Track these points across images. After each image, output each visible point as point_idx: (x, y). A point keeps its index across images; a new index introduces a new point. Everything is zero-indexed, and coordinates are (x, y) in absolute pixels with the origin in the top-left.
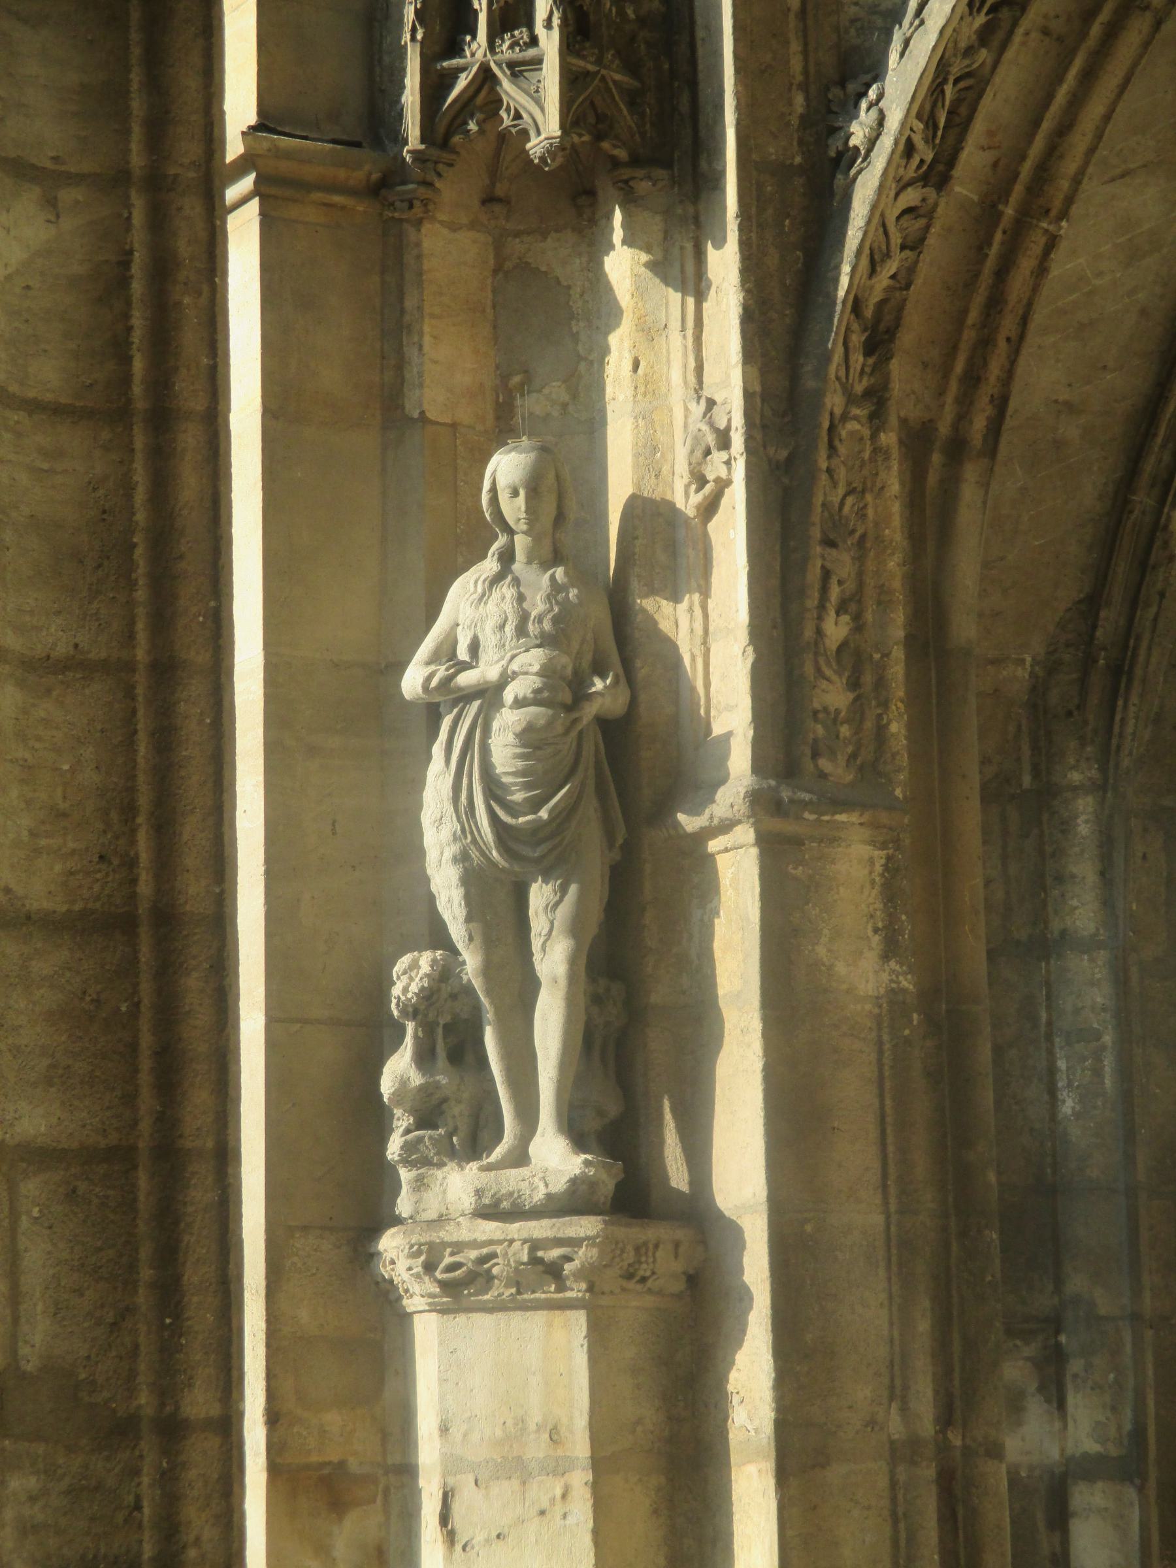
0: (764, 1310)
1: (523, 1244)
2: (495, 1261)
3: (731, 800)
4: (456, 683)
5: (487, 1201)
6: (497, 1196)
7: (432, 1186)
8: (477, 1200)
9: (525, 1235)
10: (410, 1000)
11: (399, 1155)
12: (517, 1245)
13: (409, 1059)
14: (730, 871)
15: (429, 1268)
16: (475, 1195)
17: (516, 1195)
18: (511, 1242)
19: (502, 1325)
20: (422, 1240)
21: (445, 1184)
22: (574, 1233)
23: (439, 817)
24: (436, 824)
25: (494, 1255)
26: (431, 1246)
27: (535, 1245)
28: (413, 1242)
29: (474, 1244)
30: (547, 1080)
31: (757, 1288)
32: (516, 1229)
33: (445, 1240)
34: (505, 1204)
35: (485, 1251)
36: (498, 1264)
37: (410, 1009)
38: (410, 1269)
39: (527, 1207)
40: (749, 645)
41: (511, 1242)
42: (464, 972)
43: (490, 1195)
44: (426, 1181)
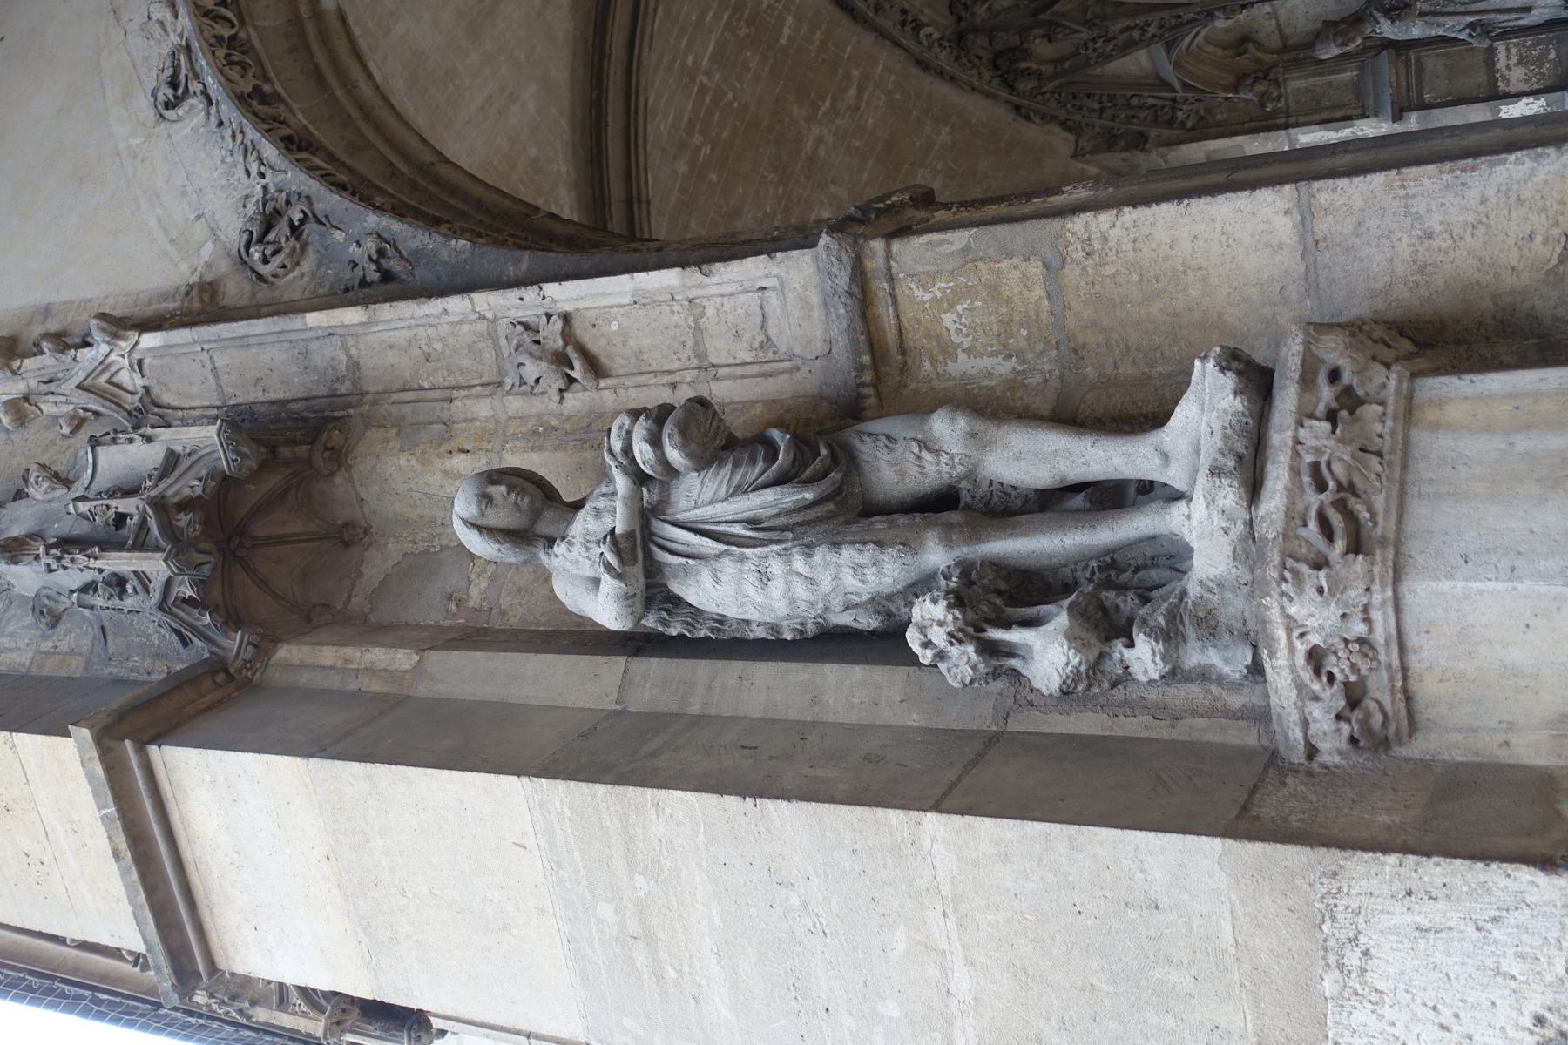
0: (1444, 177)
1: (1302, 426)
2: (1323, 466)
3: (834, 259)
4: (622, 535)
5: (1231, 463)
6: (1226, 452)
7: (1210, 606)
8: (1226, 477)
9: (1290, 421)
10: (956, 619)
11: (1157, 641)
12: (1302, 433)
13: (1034, 633)
14: (916, 292)
15: (1320, 564)
16: (1219, 477)
17: (1229, 431)
18: (1298, 442)
19: (1431, 490)
20: (1277, 560)
21: (1211, 584)
22: (1296, 359)
23: (758, 574)
24: (765, 580)
25: (1315, 466)
26: (1287, 554)
27: (1304, 415)
28: (1275, 575)
29: (1295, 490)
30: (1093, 451)
31: (1414, 196)
32: (1280, 438)
33: (1280, 530)
34: (1240, 447)
35: (1306, 479)
36: (1329, 464)
37: (970, 630)
38: (1320, 591)
39: (1250, 421)
40: (700, 269)
41: (1298, 442)
42: (946, 570)
43: (1224, 460)
44: (1201, 615)
